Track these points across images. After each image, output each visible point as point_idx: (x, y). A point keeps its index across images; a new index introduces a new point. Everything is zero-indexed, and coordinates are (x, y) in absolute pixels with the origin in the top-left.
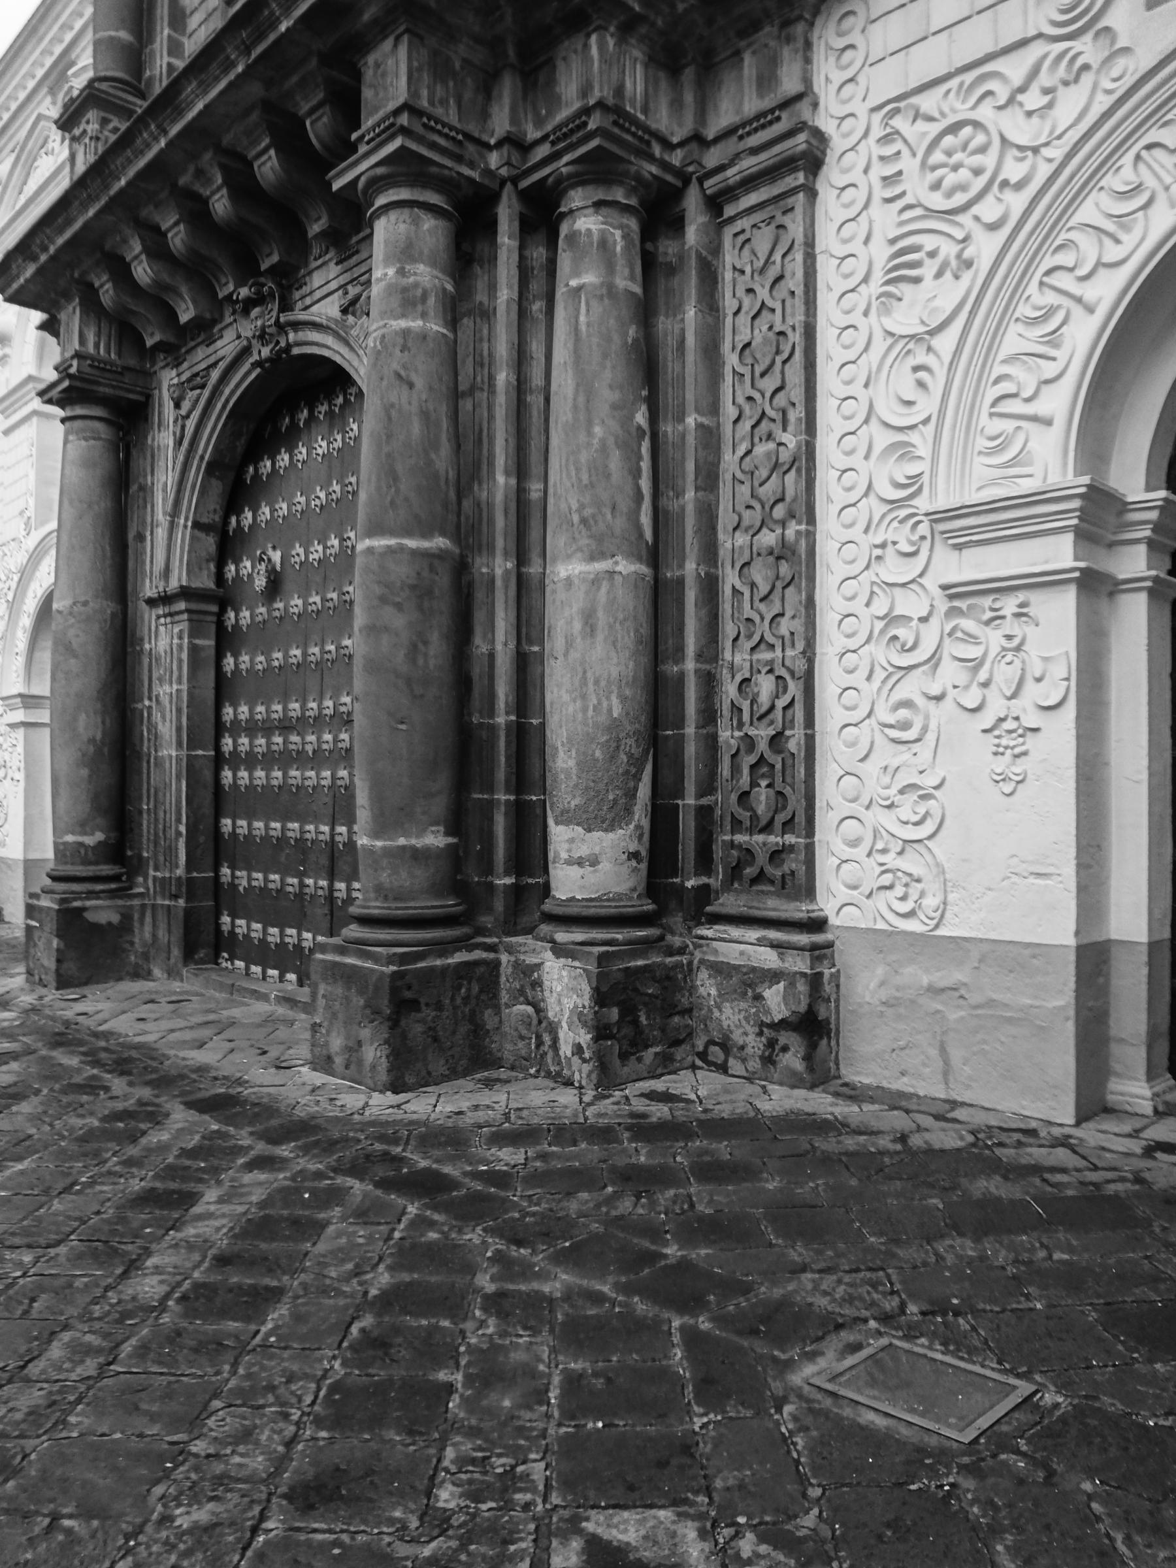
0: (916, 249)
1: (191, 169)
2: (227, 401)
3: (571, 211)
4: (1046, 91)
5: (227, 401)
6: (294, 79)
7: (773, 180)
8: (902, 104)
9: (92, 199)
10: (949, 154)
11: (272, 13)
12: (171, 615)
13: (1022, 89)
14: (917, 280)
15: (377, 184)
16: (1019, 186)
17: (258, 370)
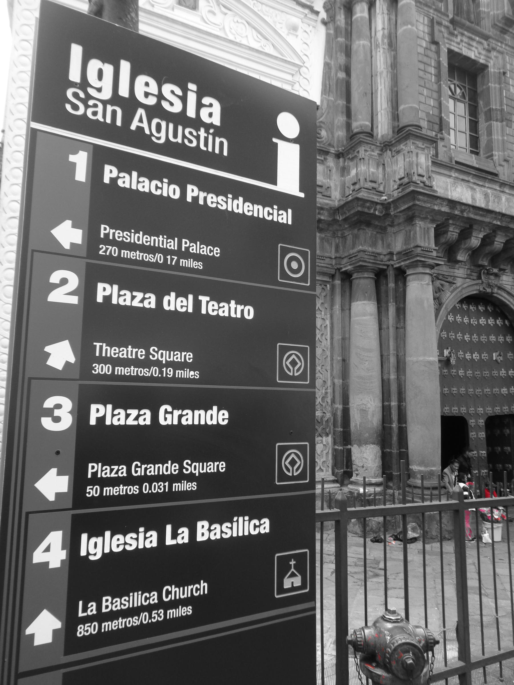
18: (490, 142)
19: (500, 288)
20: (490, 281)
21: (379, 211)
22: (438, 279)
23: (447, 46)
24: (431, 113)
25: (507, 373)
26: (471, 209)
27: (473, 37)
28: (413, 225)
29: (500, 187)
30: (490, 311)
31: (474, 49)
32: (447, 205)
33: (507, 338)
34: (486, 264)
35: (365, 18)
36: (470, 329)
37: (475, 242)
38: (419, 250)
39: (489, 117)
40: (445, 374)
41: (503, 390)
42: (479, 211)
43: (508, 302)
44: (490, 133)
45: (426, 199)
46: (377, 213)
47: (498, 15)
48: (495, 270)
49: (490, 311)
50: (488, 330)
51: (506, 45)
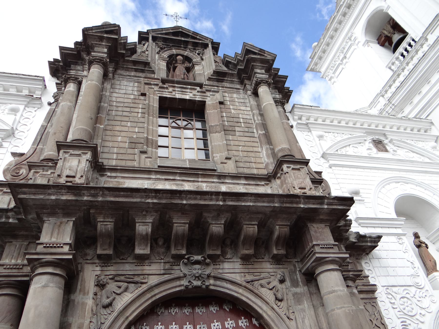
0: (405, 322)
2: (155, 295)
3: (351, 286)
4: (420, 298)
5: (155, 295)
7: (367, 294)
8: (389, 288)
9: (155, 198)
10: (404, 303)
11: (300, 201)
13: (414, 295)
15: (333, 262)
16: (423, 315)
17: (183, 288)
19: (216, 278)
20: (194, 272)
21: (13, 218)
22: (117, 281)
23: (159, 95)
24: (135, 136)
26: (106, 192)
27: (185, 86)
30: (228, 310)
31: (188, 93)
32: (68, 192)
34: (184, 253)
35: (70, 90)
37: (143, 227)
39: (210, 133)
43: (236, 294)
44: (211, 143)
45: (33, 190)
46: (11, 220)
47: (210, 73)
48: (199, 258)
49: (228, 310)
51: (223, 87)
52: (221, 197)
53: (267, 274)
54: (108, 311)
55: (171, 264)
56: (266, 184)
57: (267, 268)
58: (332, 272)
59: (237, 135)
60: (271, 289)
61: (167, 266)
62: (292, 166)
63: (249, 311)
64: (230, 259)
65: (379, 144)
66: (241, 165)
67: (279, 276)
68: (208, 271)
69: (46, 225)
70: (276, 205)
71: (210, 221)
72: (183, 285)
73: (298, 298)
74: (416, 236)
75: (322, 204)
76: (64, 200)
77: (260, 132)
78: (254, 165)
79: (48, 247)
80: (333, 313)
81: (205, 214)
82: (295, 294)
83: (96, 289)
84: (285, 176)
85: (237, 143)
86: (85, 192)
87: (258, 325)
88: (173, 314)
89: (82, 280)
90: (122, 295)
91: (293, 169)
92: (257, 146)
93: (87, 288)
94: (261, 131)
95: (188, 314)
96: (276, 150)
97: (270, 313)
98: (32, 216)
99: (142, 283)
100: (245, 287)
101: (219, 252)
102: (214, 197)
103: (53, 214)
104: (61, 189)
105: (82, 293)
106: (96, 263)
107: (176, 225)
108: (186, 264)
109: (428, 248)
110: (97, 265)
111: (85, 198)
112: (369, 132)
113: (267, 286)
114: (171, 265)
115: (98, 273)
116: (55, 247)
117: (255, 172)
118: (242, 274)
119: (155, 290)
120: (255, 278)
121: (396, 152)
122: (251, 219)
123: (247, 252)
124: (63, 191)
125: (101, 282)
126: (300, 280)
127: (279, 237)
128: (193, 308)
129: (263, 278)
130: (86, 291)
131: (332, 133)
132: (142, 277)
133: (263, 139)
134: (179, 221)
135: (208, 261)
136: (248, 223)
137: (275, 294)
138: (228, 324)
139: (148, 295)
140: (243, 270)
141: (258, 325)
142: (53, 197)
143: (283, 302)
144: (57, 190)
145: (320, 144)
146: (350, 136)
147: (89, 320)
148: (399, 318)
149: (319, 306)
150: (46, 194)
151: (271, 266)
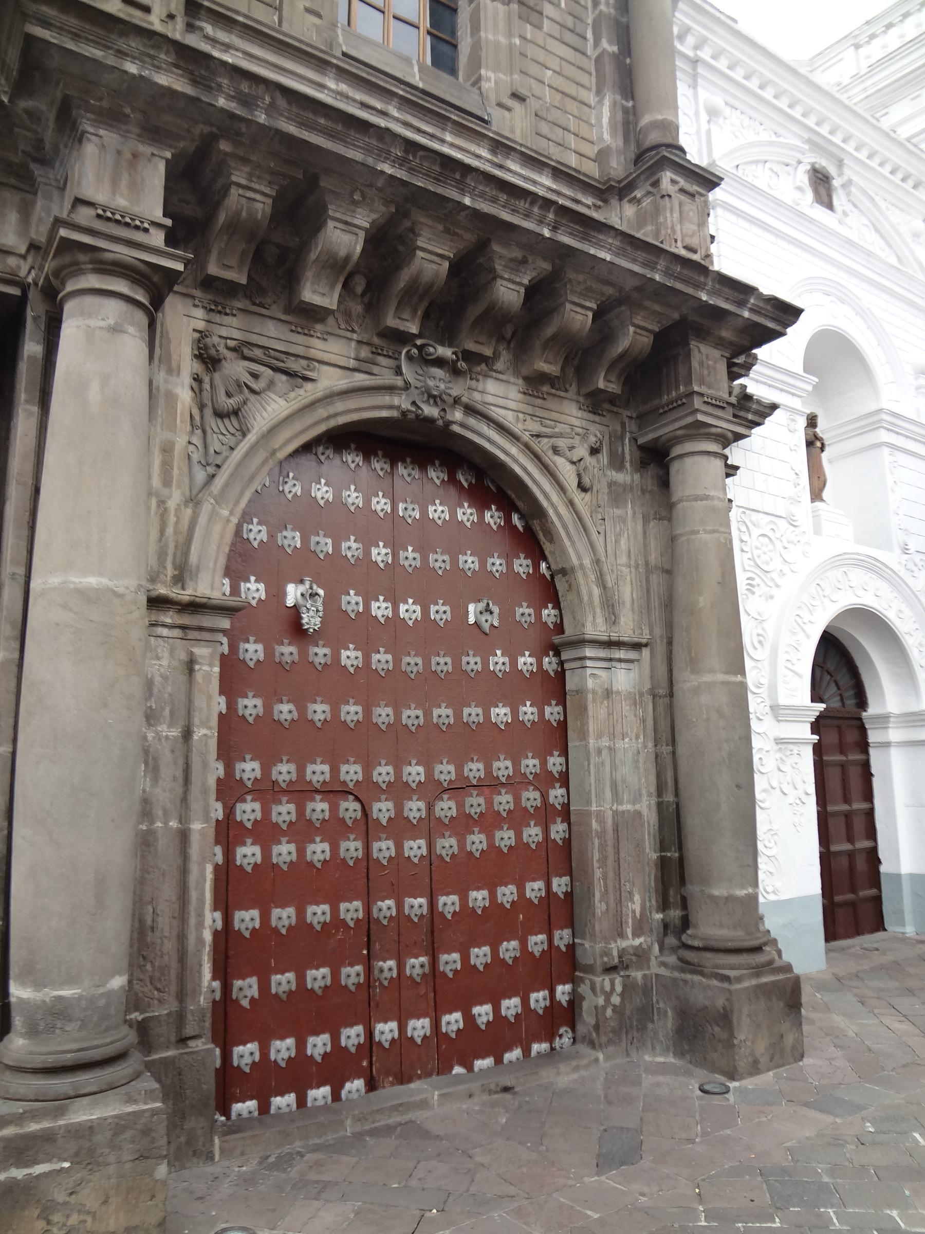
1: (516, 253)
6: (657, 307)
8: (748, 512)
9: (401, 162)
11: (705, 284)
12: (183, 628)
14: (753, 593)
17: (395, 414)
18: (476, 46)
19: (470, 410)
20: (431, 383)
25: (514, 663)
26: (281, 102)
28: (80, 141)
29: (493, 151)
32: (177, 66)
33: (517, 562)
34: (414, 329)
36: (394, 531)
37: (344, 235)
38: (84, 216)
40: (288, 659)
41: (497, 710)
42: (315, 112)
43: (502, 456)
48: (445, 352)
50: (453, 538)
52: (551, 216)
53: (567, 429)
54: (231, 424)
55: (374, 350)
56: (595, 205)
57: (571, 415)
58: (712, 458)
59: (545, 29)
60: (573, 463)
61: (365, 353)
62: (682, 182)
63: (513, 496)
64: (500, 372)
65: (821, 184)
66: (545, 128)
67: (592, 439)
68: (457, 389)
69: (90, 149)
70: (657, 277)
71: (499, 268)
72: (398, 408)
73: (617, 494)
74: (812, 421)
75: (741, 304)
76: (162, 87)
77: (605, 44)
78: (572, 141)
79: (108, 219)
80: (693, 537)
81: (496, 247)
82: (611, 484)
83: (198, 367)
84: (661, 202)
85: (541, 56)
86: (225, 82)
87: (521, 529)
88: (352, 466)
89: (162, 332)
90: (263, 395)
91: (682, 190)
92: (587, 84)
93: (175, 357)
94: (610, 43)
95: (381, 473)
96: (646, 120)
97: (563, 510)
98: (41, 104)
99: (306, 379)
100: (527, 446)
101: (488, 352)
102: (536, 210)
103: (112, 118)
104: (157, 47)
105: (164, 368)
106: (193, 297)
107: (420, 254)
108: (410, 358)
109: (823, 451)
110: (197, 302)
111: (221, 102)
112: (816, 144)
113: (568, 453)
114: (373, 353)
115: (201, 325)
116: (127, 225)
117: (573, 161)
118: (521, 415)
119: (337, 404)
120: (544, 429)
121: (847, 220)
122: (587, 292)
123: (546, 367)
124: (162, 56)
125: (213, 352)
126: (628, 457)
127: (622, 356)
128: (393, 465)
129: (561, 435)
130: (174, 364)
131: (738, 112)
132: (304, 363)
133: (609, 69)
134: (430, 248)
135: (462, 365)
136: (576, 300)
137: (579, 475)
138: (464, 514)
139: (322, 412)
140: (522, 407)
141: (521, 529)
142: (132, 68)
143: (589, 494)
144: (145, 45)
145: (709, 133)
146: (774, 138)
147: (186, 438)
148: (745, 571)
149: (651, 517)
150: (110, 48)
151: (579, 414)
